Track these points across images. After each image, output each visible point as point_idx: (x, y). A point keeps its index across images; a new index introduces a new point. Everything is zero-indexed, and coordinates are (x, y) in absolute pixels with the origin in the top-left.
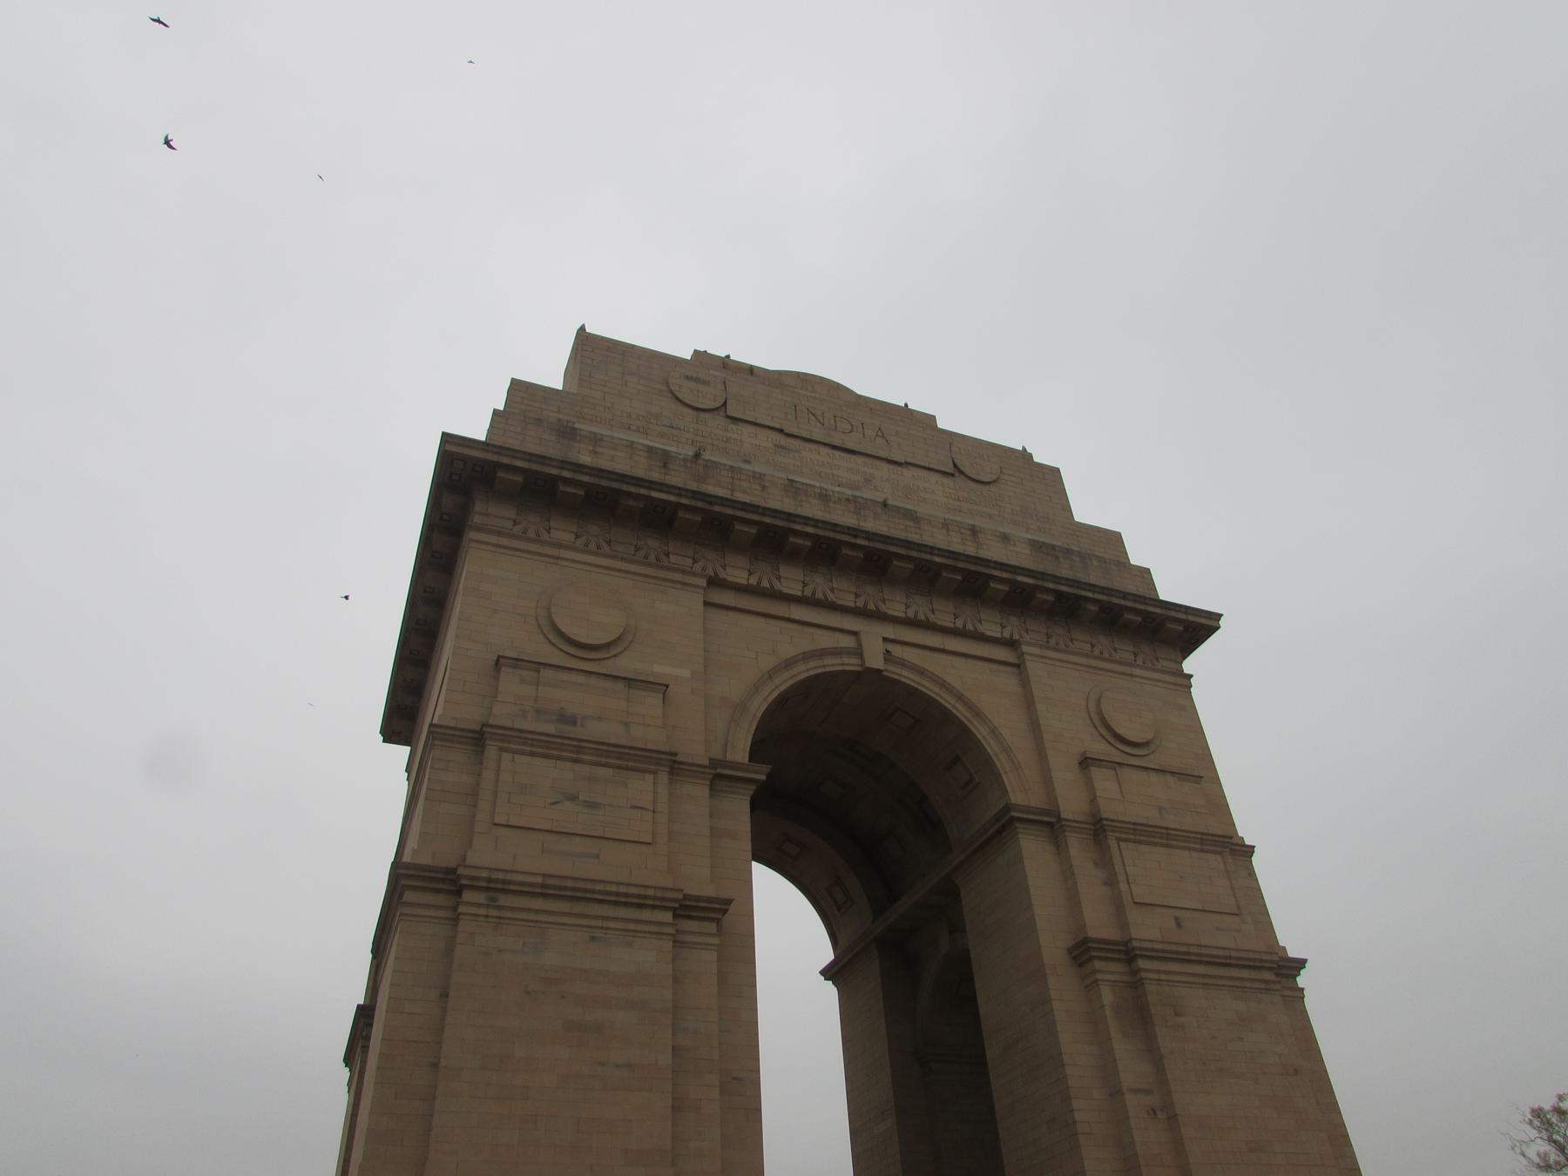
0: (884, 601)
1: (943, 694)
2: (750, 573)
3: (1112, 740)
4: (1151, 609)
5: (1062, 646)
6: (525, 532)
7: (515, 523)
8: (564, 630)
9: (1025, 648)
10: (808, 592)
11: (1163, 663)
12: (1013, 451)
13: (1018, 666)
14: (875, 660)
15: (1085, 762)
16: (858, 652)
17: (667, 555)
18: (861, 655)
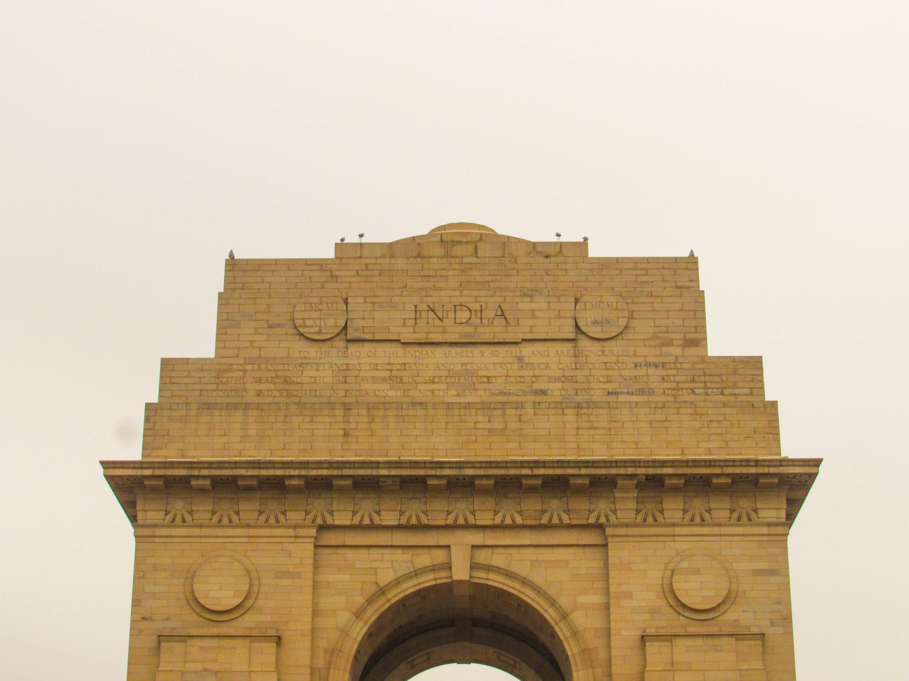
0: (473, 513)
1: (523, 589)
2: (354, 513)
3: (680, 610)
4: (738, 470)
5: (650, 520)
6: (173, 521)
7: (167, 513)
8: (202, 601)
9: (609, 531)
10: (404, 521)
11: (761, 513)
12: (676, 260)
13: (606, 546)
14: (460, 573)
15: (643, 639)
16: (448, 566)
17: (284, 513)
18: (450, 568)
